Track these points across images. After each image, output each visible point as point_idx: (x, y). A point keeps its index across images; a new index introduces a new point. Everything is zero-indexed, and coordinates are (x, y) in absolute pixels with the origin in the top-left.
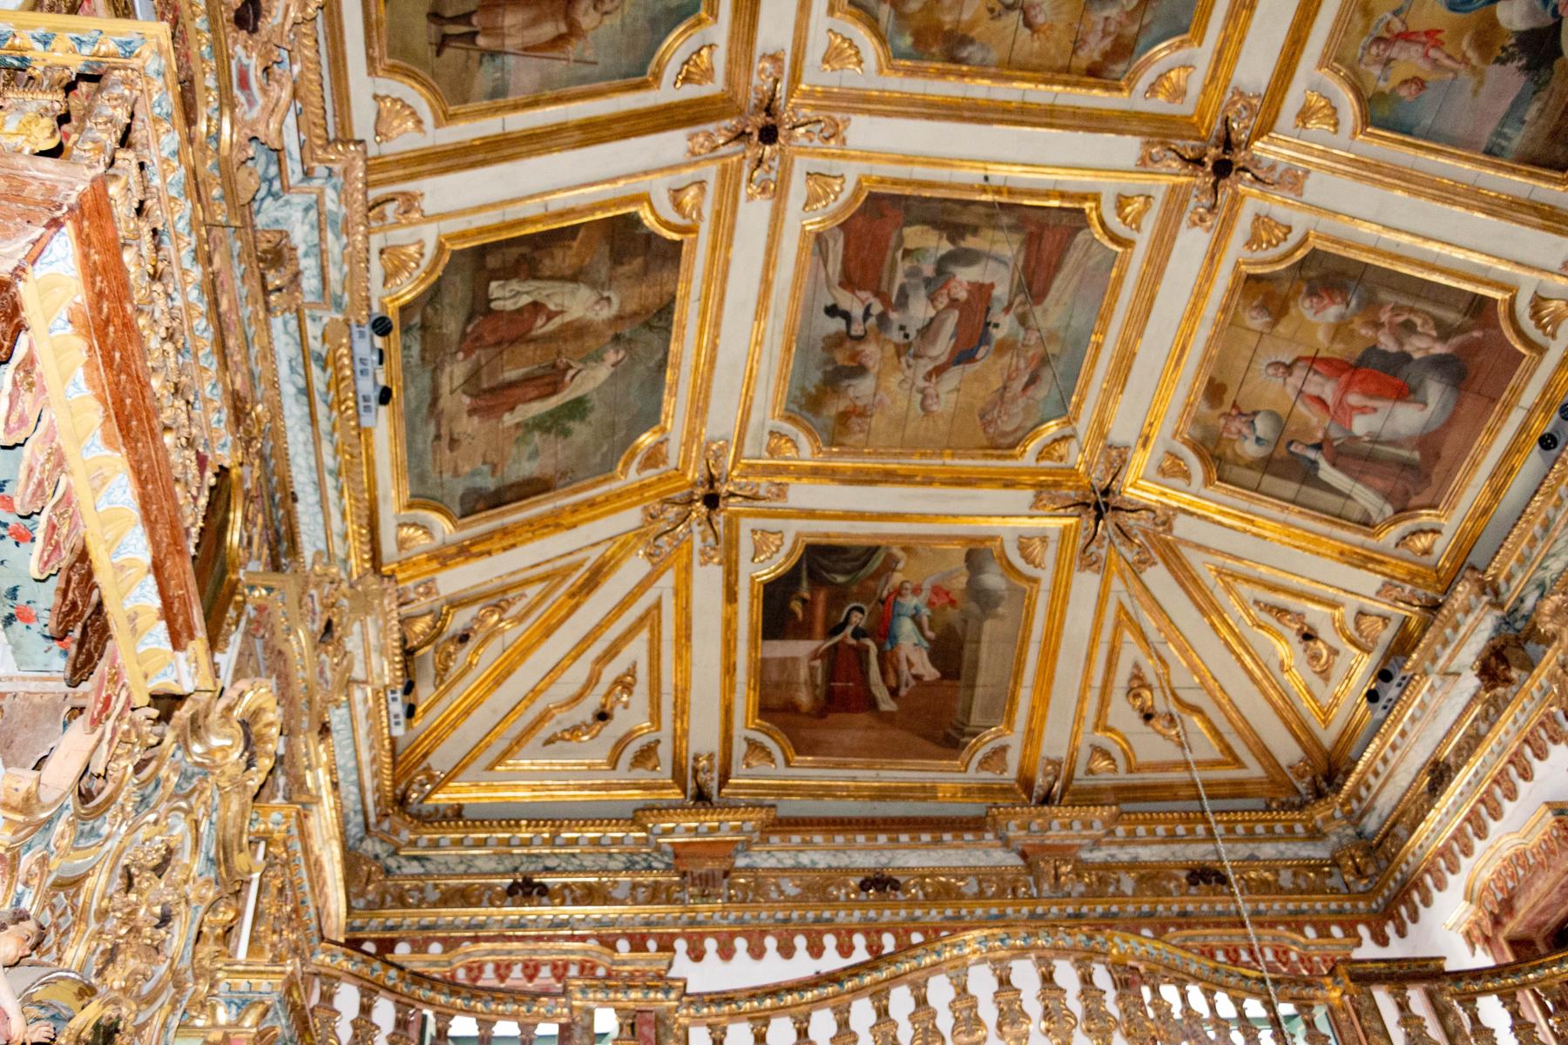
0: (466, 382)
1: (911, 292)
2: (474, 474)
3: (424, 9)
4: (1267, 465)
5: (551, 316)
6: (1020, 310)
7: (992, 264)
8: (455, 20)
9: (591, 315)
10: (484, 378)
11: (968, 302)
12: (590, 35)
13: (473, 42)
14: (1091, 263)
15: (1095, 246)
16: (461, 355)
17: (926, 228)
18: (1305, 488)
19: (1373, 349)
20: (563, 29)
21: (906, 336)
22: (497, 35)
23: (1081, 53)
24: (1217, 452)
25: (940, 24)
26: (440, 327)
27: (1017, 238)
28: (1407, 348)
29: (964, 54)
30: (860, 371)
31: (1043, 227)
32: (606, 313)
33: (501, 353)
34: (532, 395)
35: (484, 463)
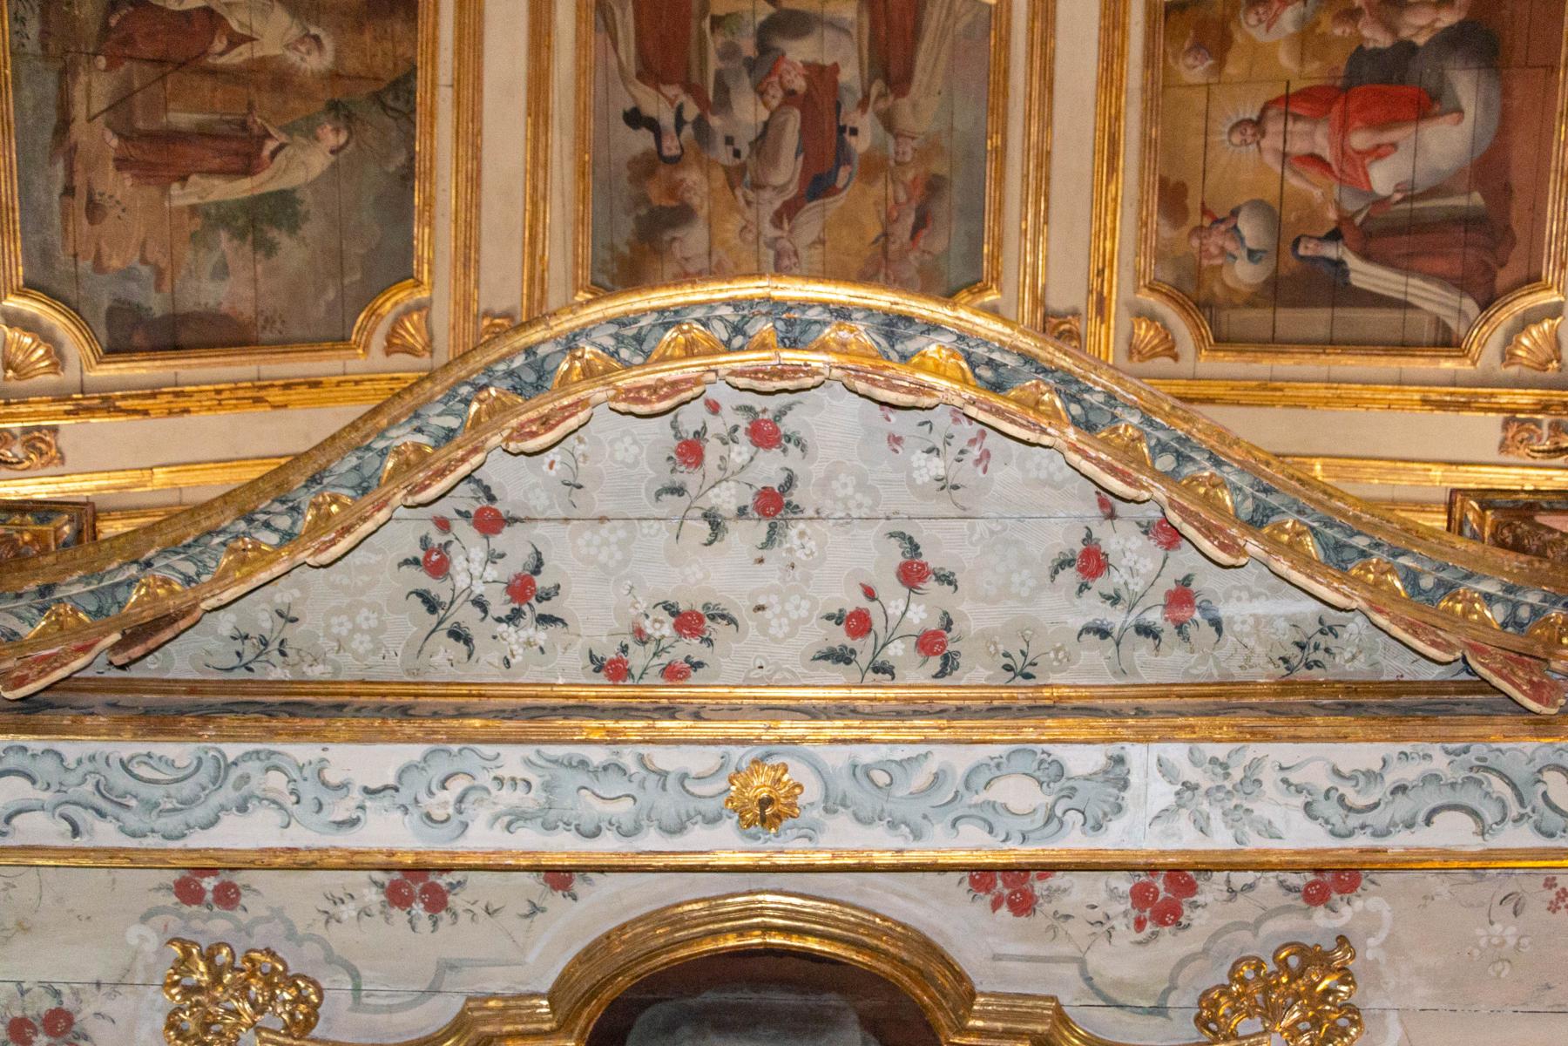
0: (110, 108)
1: (731, 83)
2: (127, 274)
4: (1276, 292)
5: (235, 41)
6: (882, 105)
7: (830, 35)
9: (293, 57)
10: (139, 112)
11: (808, 95)
16: (102, 62)
18: (1340, 313)
19: (1361, 55)
21: (737, 154)
24: (1203, 295)
28: (1405, 33)
30: (683, 214)
32: (315, 62)
33: (163, 77)
34: (216, 163)
35: (144, 261)
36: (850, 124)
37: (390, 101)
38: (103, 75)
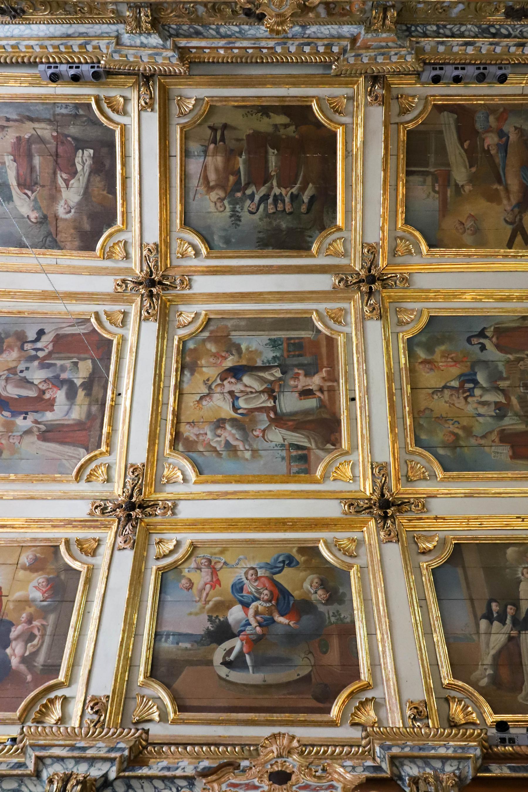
0: (39, 136)
3: (229, 122)
5: (67, 182)
6: (35, 429)
7: (66, 408)
8: (223, 135)
9: (62, 203)
10: (38, 146)
11: (44, 399)
12: (208, 197)
13: (212, 143)
14: (64, 462)
15: (75, 461)
16: (55, 134)
17: (91, 370)
20: (212, 184)
22: (213, 153)
23: (188, 426)
25: (199, 358)
26: (74, 124)
27: (83, 417)
29: (186, 372)
31: (89, 429)
32: (61, 211)
33: (51, 155)
34: (21, 172)
36: (28, 416)
37: (49, 239)
38: (50, 134)
